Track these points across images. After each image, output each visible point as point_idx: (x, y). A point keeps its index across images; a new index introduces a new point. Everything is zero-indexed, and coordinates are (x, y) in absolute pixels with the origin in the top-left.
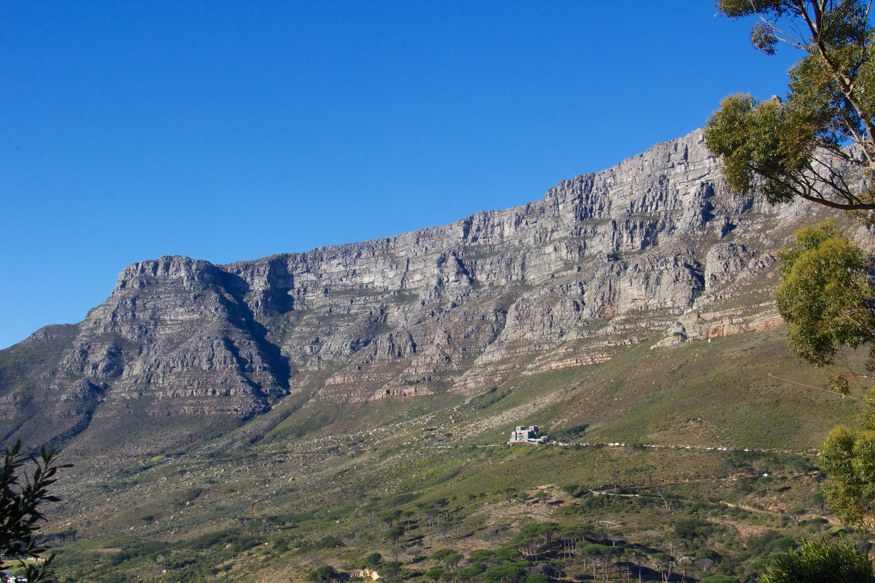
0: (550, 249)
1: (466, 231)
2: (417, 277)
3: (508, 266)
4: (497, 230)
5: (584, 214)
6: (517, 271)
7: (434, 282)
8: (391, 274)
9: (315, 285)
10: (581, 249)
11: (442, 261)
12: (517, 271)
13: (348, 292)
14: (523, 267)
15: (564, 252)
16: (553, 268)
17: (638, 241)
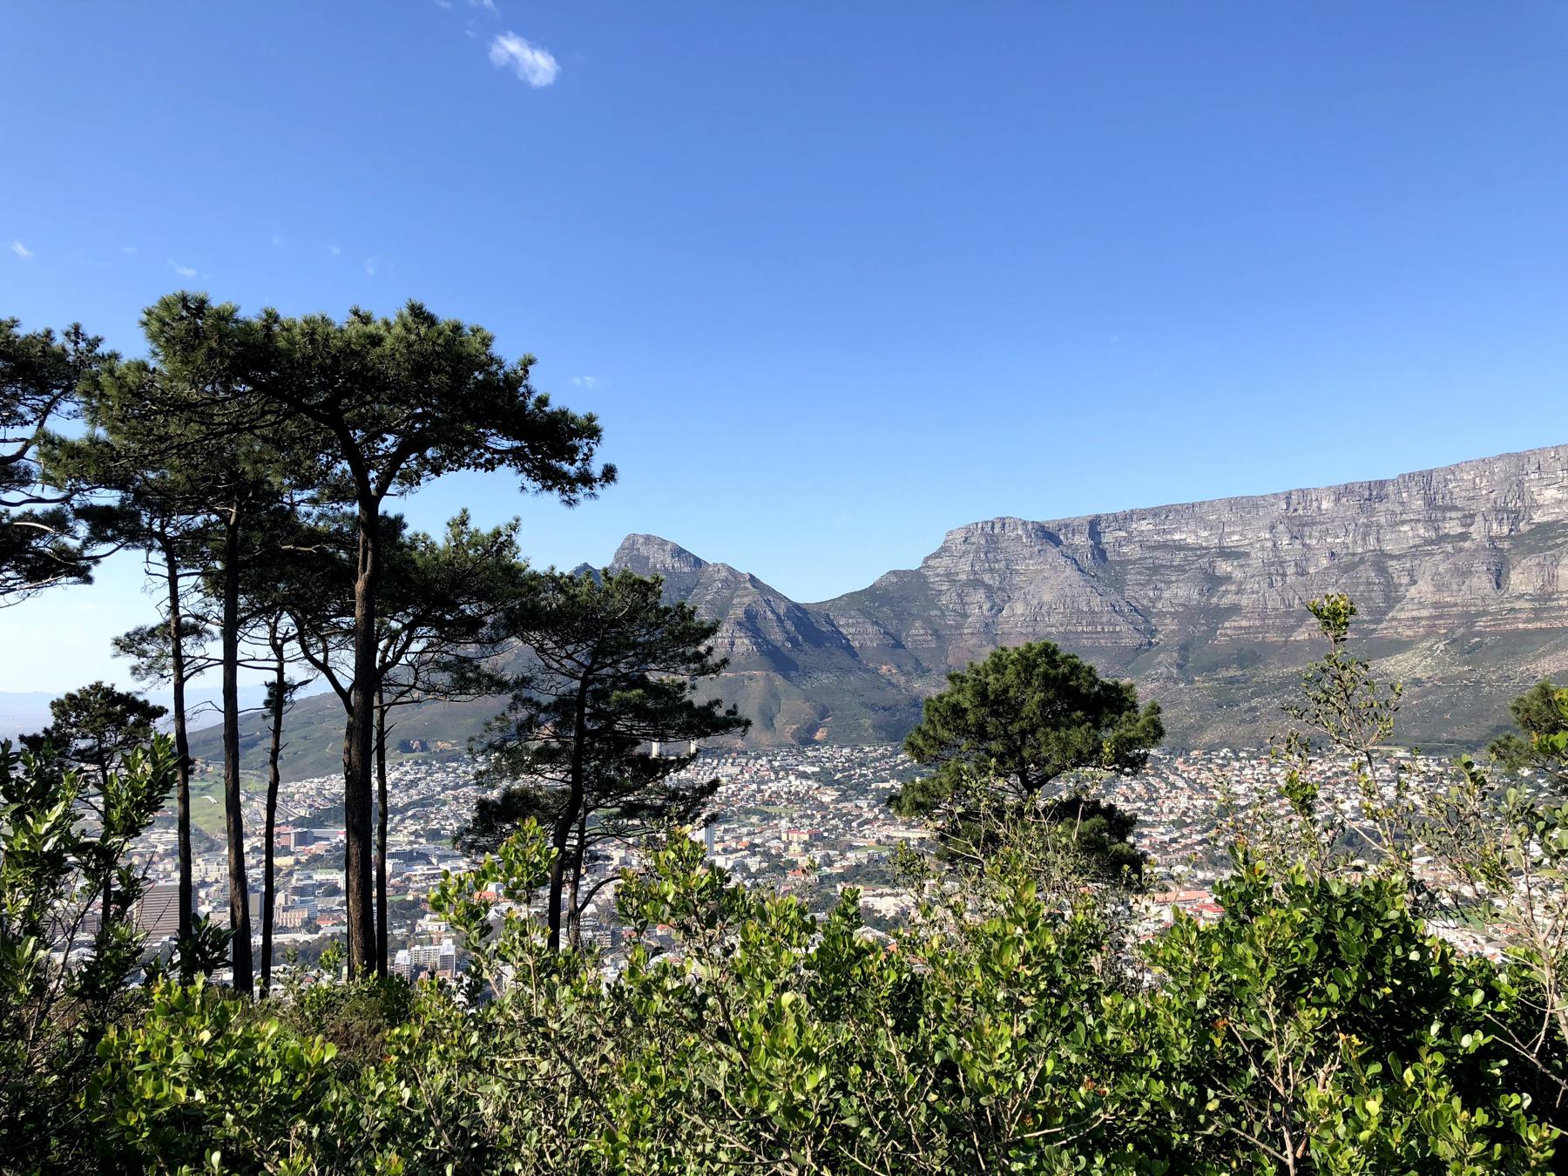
0: (1406, 528)
1: (1288, 504)
2: (1235, 538)
3: (1364, 539)
4: (1315, 504)
5: (1430, 503)
6: (1372, 540)
7: (1269, 544)
8: (1205, 534)
9: (1129, 540)
10: (1437, 529)
11: (1273, 527)
12: (1372, 540)
13: (1164, 546)
14: (1378, 540)
15: (1421, 532)
16: (1411, 543)
17: (1506, 530)
